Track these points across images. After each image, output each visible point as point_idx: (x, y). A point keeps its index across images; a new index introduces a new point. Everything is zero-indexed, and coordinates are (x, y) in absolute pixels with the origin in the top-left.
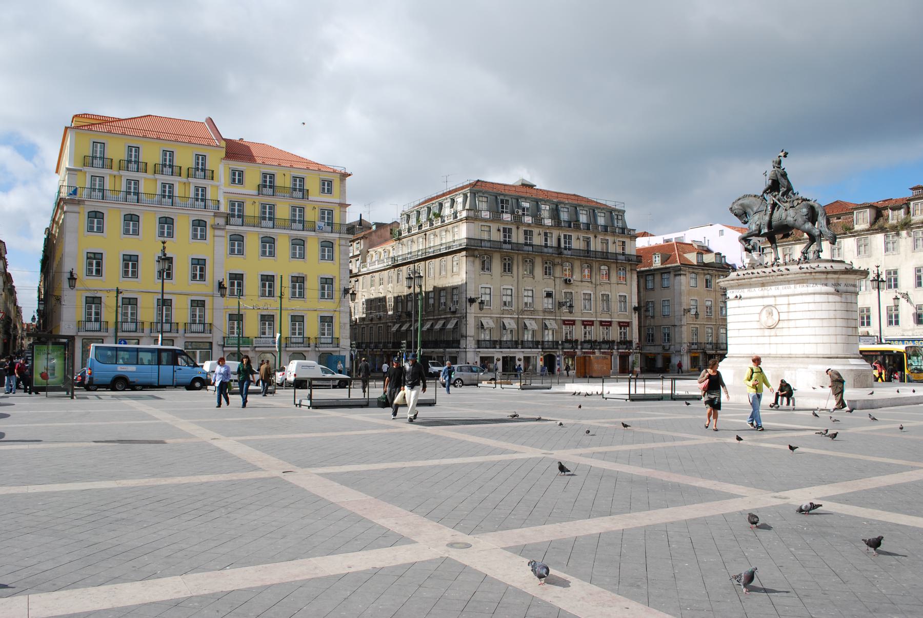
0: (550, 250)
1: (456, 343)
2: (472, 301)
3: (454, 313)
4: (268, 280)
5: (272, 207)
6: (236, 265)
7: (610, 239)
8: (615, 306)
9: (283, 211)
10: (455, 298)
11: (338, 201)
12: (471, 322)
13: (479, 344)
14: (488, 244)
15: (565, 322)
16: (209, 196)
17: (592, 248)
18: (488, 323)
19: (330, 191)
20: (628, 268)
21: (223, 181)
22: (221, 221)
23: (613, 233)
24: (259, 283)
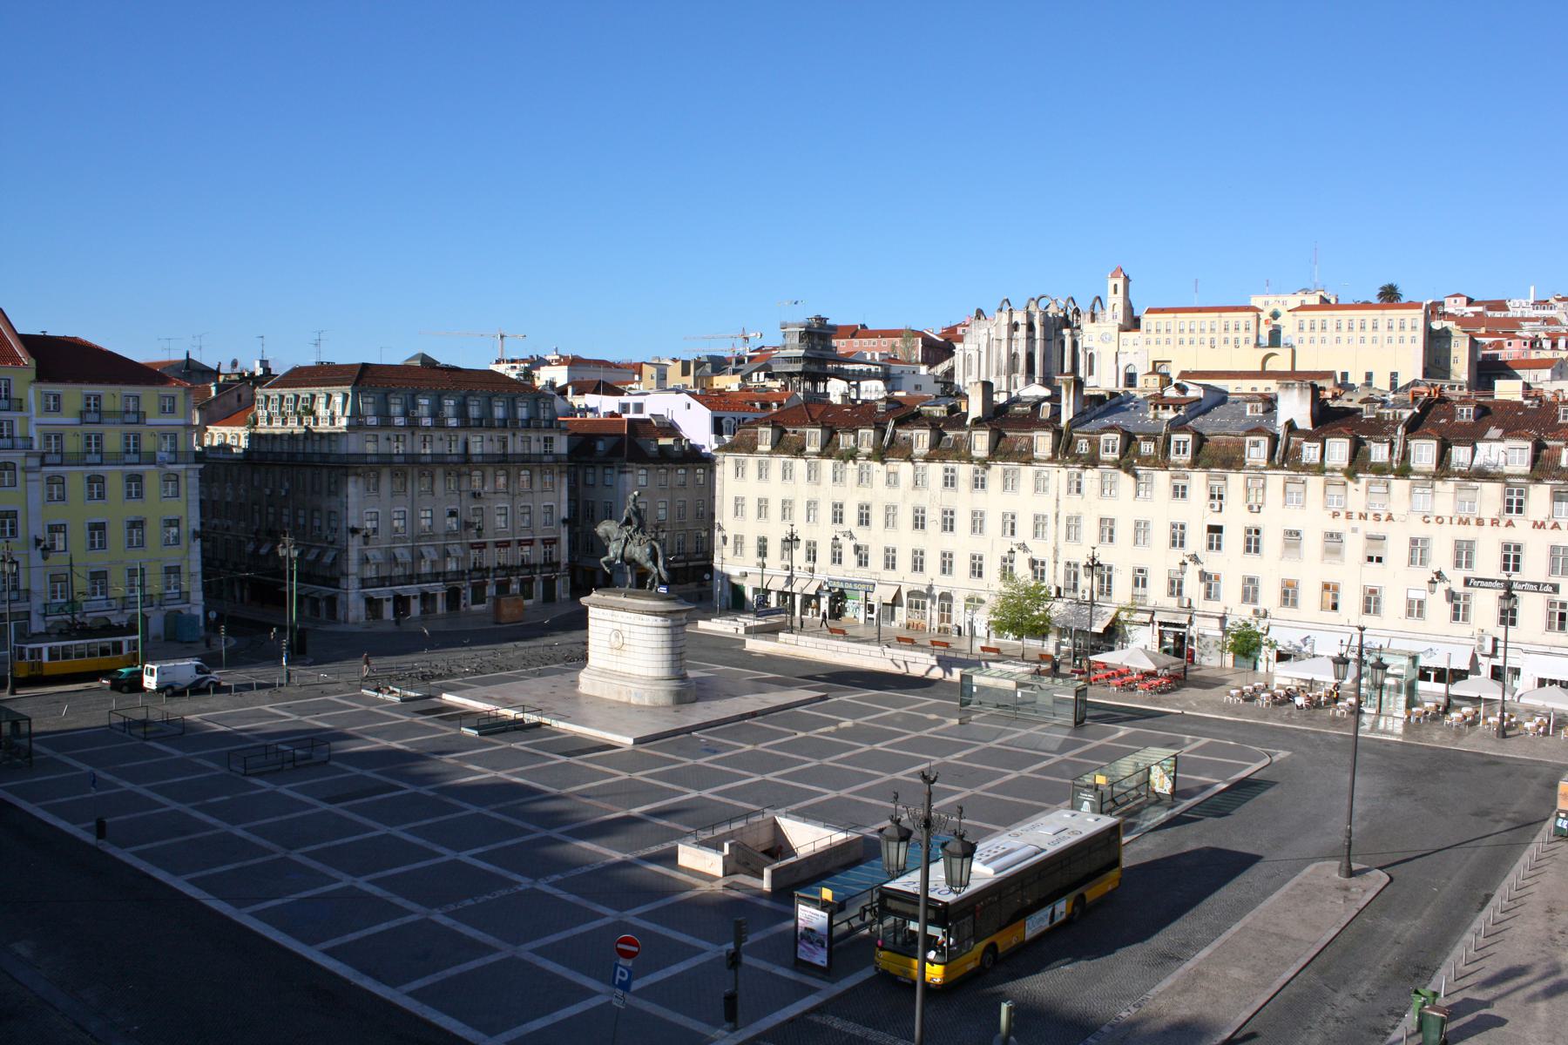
0: (455, 459)
1: (334, 582)
2: (354, 531)
3: (332, 543)
4: (98, 528)
5: (99, 437)
6: (57, 513)
7: (533, 435)
8: (539, 519)
9: (113, 439)
10: (333, 524)
11: (182, 421)
12: (353, 555)
13: (364, 583)
14: (375, 459)
15: (473, 546)
16: (17, 433)
17: (510, 450)
18: (374, 554)
19: (172, 410)
20: (556, 470)
21: (34, 410)
22: (34, 462)
23: (538, 428)
24: (87, 534)
